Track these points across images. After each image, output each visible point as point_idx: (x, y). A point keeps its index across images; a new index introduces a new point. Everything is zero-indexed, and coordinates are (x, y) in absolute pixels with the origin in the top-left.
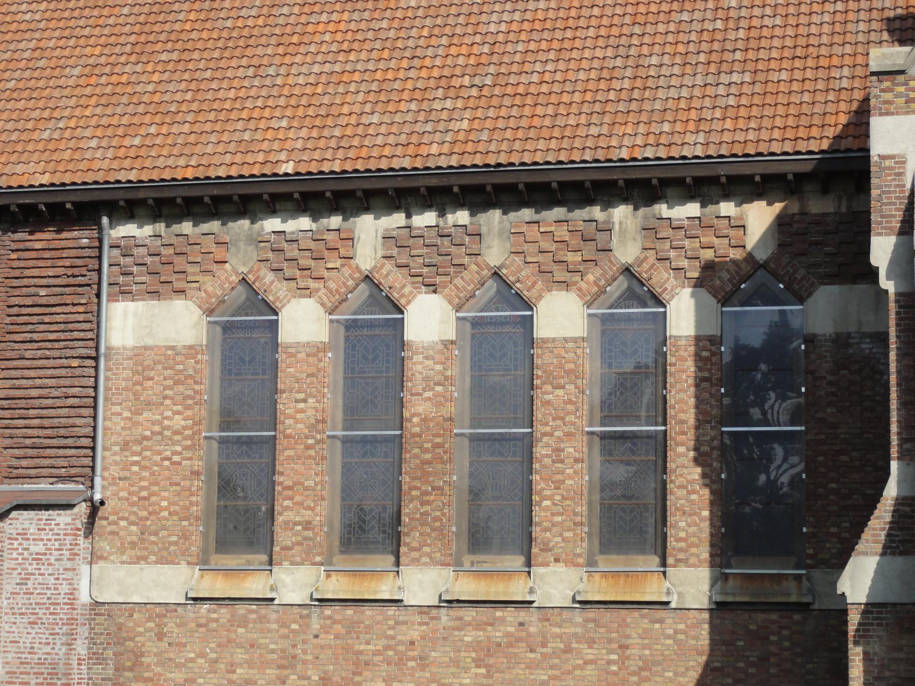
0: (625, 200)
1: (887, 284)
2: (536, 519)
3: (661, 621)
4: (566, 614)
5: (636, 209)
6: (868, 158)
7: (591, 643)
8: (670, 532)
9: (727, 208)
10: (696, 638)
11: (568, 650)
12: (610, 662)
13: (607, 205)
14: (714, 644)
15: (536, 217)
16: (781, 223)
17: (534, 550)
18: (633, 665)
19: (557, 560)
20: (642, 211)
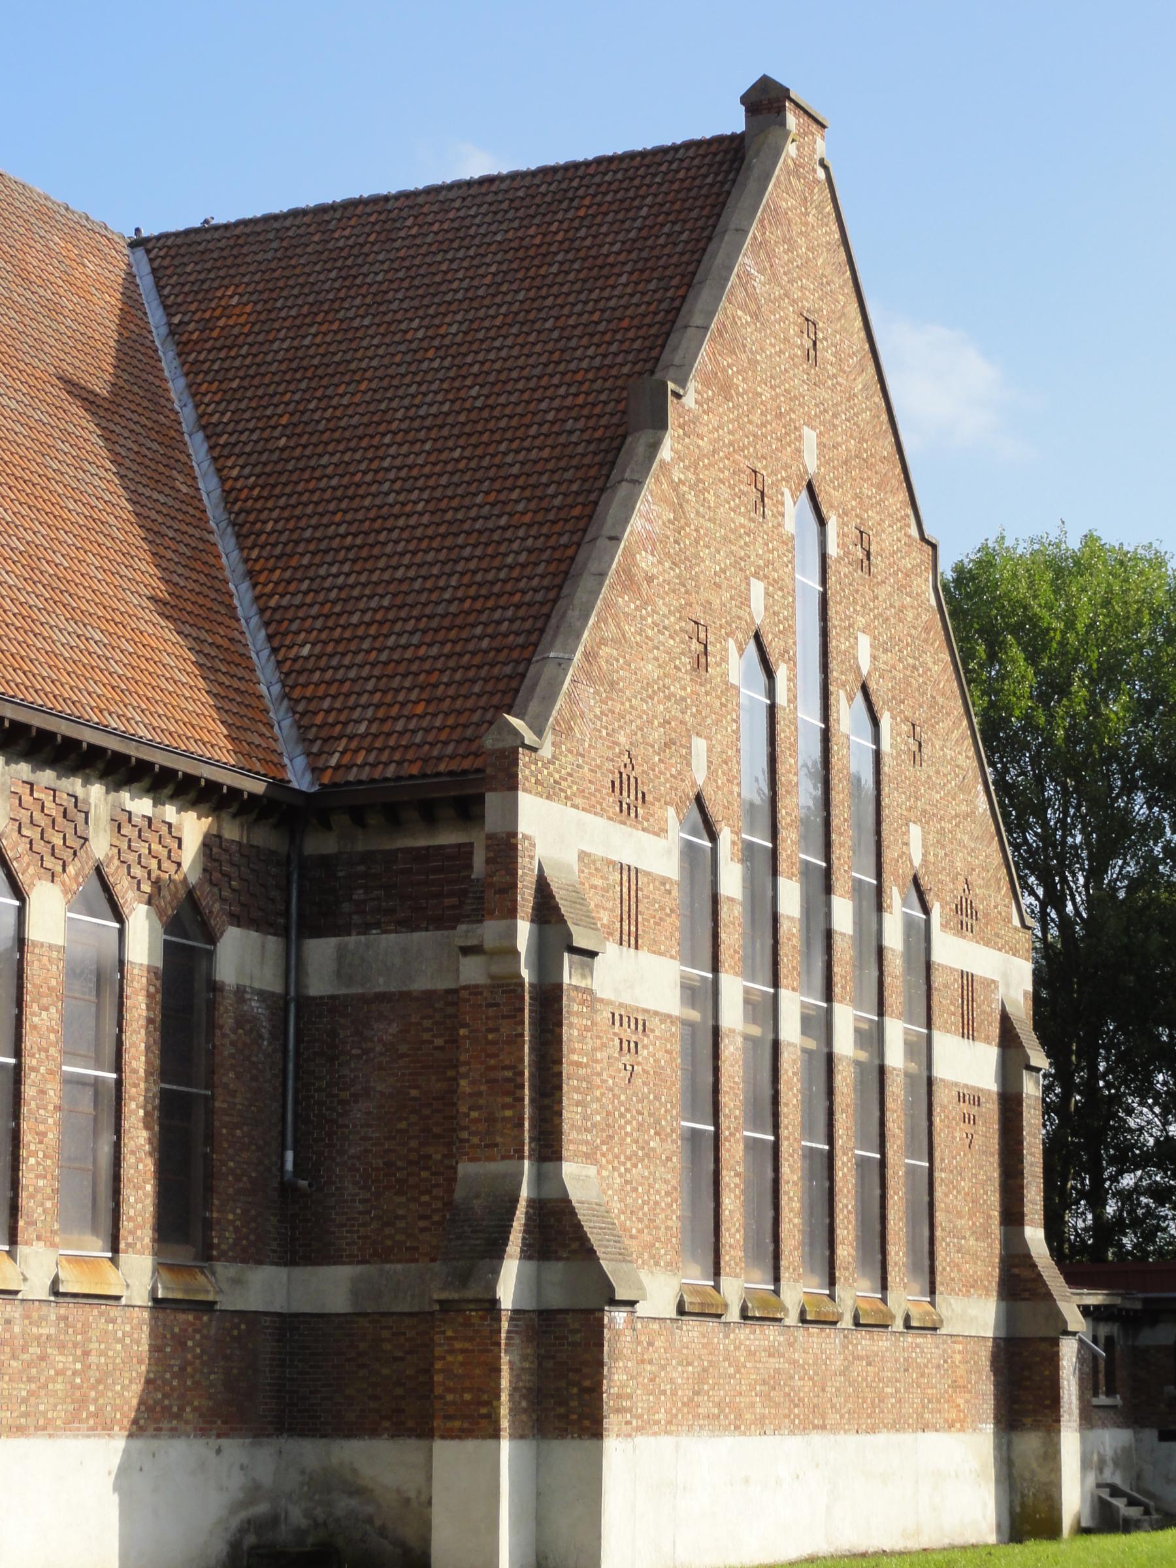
0: (103, 776)
1: (525, 973)
2: (24, 1181)
3: (113, 1321)
4: (45, 1309)
5: (107, 792)
6: (515, 835)
7: (62, 1346)
8: (124, 1208)
9: (170, 812)
10: (138, 1343)
11: (43, 1358)
12: (75, 1373)
13: (86, 782)
14: (155, 1349)
15: (31, 777)
16: (210, 845)
17: (21, 1223)
18: (93, 1374)
19: (39, 1238)
20: (113, 795)
